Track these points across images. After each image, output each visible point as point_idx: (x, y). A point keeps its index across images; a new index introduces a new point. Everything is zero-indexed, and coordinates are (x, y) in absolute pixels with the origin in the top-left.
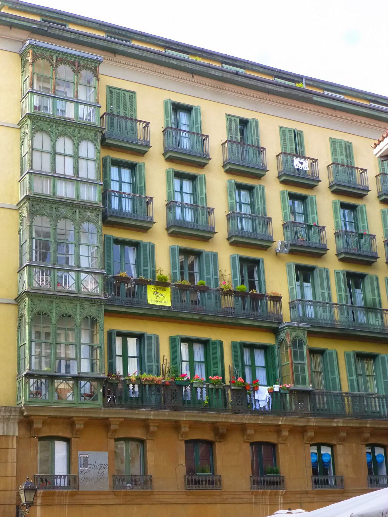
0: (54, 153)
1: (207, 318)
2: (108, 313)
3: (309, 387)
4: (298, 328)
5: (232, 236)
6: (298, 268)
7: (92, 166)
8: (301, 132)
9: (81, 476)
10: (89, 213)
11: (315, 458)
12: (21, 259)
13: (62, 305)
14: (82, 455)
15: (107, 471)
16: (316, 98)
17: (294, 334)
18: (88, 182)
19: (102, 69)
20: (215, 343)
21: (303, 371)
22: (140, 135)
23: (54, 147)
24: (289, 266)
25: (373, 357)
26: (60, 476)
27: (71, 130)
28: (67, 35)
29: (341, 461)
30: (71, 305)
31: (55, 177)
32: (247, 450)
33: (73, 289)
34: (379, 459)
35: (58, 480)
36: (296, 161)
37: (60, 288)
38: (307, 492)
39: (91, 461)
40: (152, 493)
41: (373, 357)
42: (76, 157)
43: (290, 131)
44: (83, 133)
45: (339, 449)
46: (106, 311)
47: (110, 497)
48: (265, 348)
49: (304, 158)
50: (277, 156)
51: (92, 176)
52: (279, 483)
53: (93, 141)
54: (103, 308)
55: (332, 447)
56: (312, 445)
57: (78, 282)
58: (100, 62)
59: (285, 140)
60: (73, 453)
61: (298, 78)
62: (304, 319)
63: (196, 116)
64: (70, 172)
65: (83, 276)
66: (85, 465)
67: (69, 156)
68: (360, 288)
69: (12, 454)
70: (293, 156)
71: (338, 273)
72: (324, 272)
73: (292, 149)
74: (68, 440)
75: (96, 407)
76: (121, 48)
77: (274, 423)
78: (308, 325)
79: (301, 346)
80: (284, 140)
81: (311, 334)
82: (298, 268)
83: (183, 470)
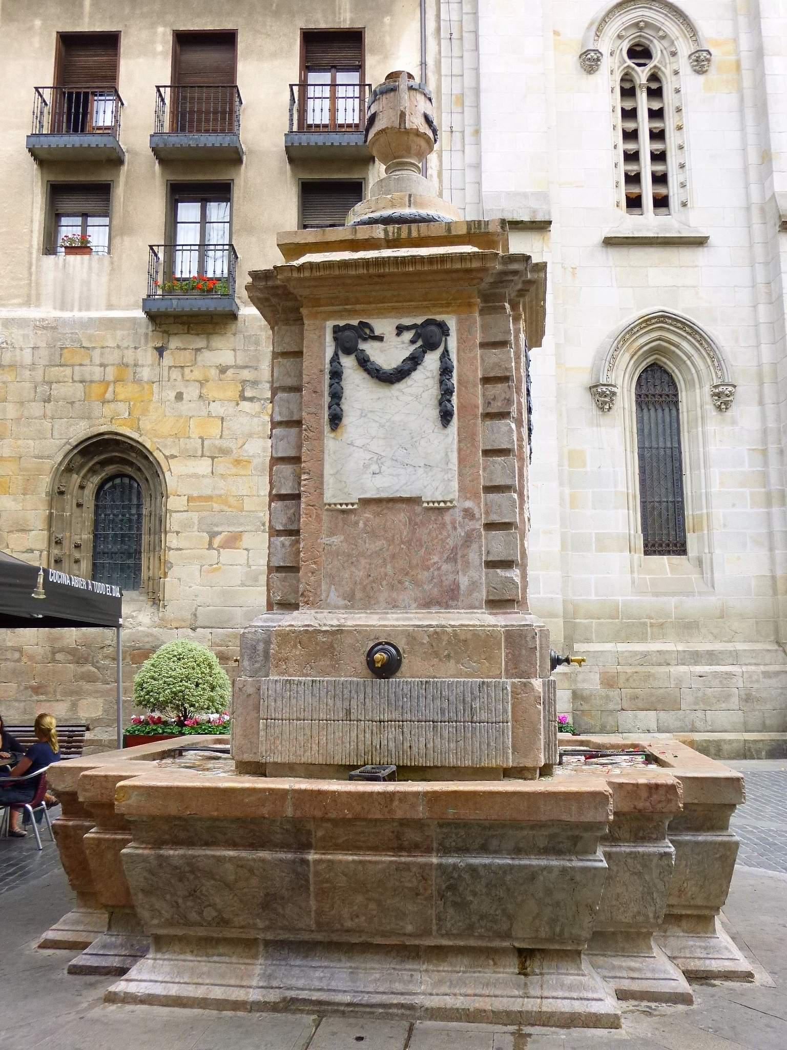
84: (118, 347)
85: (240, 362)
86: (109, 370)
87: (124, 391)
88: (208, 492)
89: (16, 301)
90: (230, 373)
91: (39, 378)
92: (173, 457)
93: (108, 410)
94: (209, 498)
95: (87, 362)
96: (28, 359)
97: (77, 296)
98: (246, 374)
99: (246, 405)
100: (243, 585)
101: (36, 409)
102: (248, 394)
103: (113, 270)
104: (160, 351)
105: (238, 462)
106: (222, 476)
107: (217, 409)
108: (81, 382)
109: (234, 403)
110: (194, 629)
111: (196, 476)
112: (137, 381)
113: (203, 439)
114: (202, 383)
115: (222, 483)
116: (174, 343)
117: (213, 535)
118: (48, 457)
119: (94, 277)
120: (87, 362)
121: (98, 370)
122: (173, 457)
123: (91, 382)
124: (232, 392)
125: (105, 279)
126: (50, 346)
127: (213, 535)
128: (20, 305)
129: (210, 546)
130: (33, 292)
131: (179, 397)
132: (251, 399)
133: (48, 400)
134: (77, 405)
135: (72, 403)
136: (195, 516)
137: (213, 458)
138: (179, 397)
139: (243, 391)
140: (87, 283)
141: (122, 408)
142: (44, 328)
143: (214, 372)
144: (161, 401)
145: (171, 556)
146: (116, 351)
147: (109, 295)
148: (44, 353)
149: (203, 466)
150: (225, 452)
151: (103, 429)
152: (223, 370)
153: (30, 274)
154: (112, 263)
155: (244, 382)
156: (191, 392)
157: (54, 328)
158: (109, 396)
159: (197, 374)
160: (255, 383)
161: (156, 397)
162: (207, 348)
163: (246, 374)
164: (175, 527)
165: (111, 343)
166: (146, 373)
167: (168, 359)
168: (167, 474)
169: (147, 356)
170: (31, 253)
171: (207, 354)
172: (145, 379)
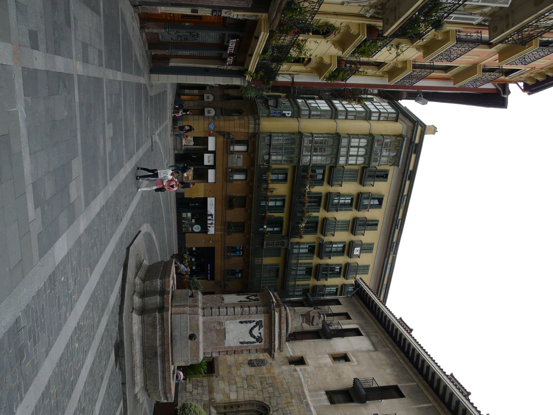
0: (358, 147)
1: (293, 207)
2: (294, 167)
3: (265, 247)
4: (288, 244)
5: (326, 220)
6: (314, 247)
7: (354, 162)
8: (372, 253)
9: (234, 156)
10: (334, 160)
11: (238, 248)
12: (316, 134)
13: (298, 149)
14: (241, 156)
15: (235, 165)
16: (386, 259)
17: (286, 242)
18: (347, 160)
19: (396, 167)
20: (283, 210)
21: (271, 245)
22: (368, 183)
23: (362, 147)
24: (314, 243)
25: (277, 276)
26: (234, 148)
27: (368, 154)
28: (410, 153)
29: (237, 258)
30: (297, 153)
31: (349, 147)
32: (242, 221)
33: (304, 153)
34: (237, 275)
35: (232, 147)
36: (358, 249)
37: (304, 148)
38: (225, 244)
39: (239, 159)
40: (227, 182)
41: (277, 276)
42: (357, 156)
43: (372, 247)
44: (367, 159)
45: (241, 258)
46: (296, 166)
47: (226, 166)
48: (281, 231)
49: (360, 253)
50: (361, 241)
51: (350, 162)
52: (229, 233)
53: (364, 163)
54: (297, 165)
55: (242, 256)
56: (243, 247)
57: (307, 156)
58: (398, 166)
59: (368, 245)
60: (242, 153)
61: (395, 253)
62: (293, 248)
63: (379, 207)
64: (351, 153)
65: (309, 157)
66: (238, 157)
67: (358, 153)
68: (306, 273)
69: (242, 130)
70: (361, 248)
71: (311, 263)
72: (312, 258)
73: (364, 248)
74: (247, 151)
75: (259, 162)
76: (405, 176)
77: (251, 232)
78: (289, 248)
79: (281, 245)
80: (368, 244)
81: (286, 249)
82: (314, 247)
83: (234, 195)
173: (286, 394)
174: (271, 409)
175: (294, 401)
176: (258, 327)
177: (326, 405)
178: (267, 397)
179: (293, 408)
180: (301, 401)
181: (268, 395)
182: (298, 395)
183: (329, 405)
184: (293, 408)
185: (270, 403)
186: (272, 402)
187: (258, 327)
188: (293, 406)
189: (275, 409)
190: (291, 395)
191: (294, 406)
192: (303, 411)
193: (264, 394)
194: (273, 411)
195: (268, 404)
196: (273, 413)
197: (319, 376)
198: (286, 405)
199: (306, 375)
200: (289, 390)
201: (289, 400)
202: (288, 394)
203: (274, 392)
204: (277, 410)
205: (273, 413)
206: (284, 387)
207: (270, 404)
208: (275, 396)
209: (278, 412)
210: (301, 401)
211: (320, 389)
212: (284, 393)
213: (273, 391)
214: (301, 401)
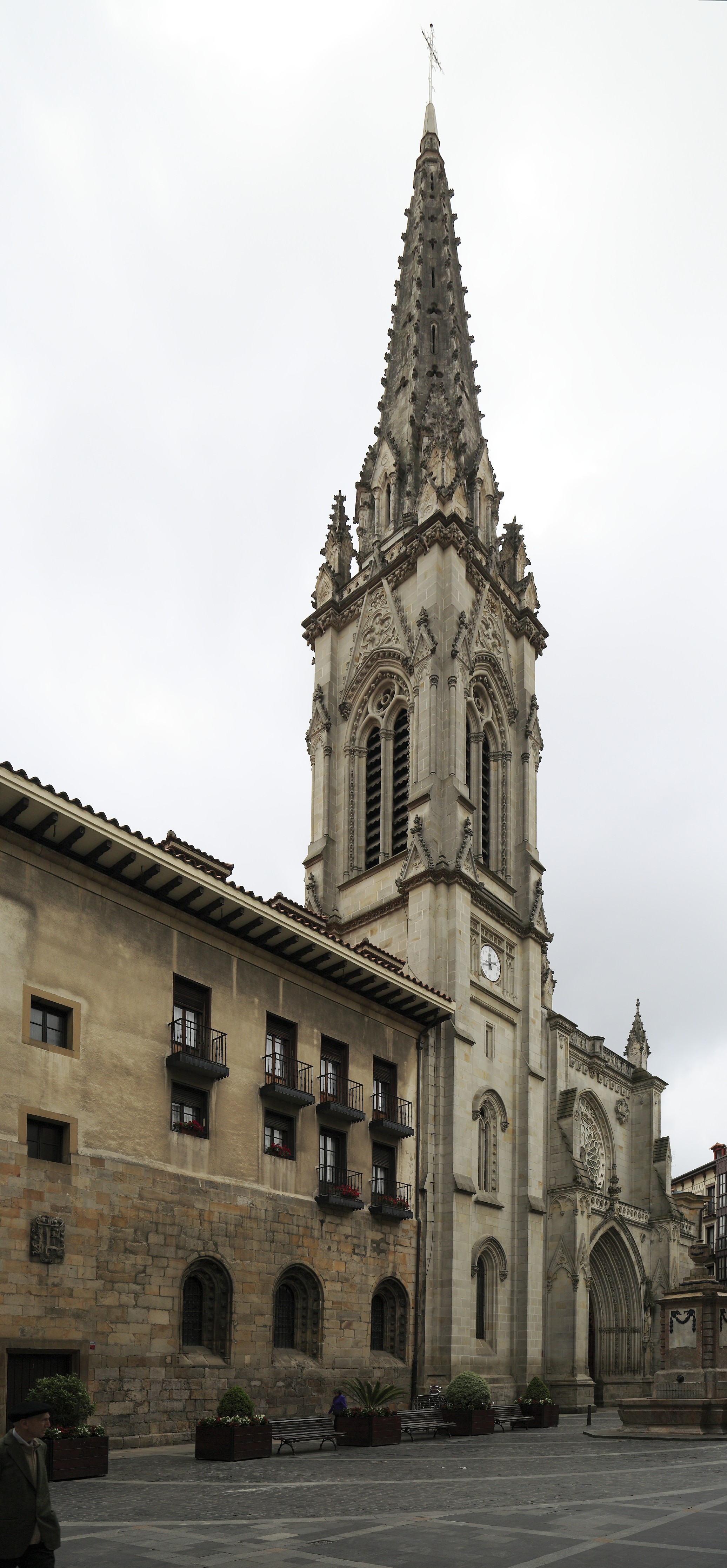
84: (304, 1217)
85: (353, 1234)
86: (301, 1229)
87: (307, 1242)
88: (340, 1300)
89: (252, 1178)
90: (349, 1239)
91: (268, 1229)
92: (327, 1280)
93: (300, 1251)
94: (340, 1303)
95: (290, 1223)
96: (263, 1217)
97: (281, 1182)
98: (355, 1241)
99: (355, 1257)
100: (352, 1347)
101: (267, 1245)
102: (356, 1251)
103: (297, 1170)
104: (322, 1222)
105: (351, 1286)
106: (346, 1293)
107: (345, 1257)
108: (288, 1233)
109: (350, 1255)
110: (333, 1369)
111: (335, 1291)
112: (312, 1237)
113: (338, 1272)
114: (339, 1242)
115: (345, 1296)
116: (328, 1219)
117: (342, 1322)
118: (273, 1274)
119: (289, 1173)
120: (290, 1223)
121: (295, 1228)
122: (327, 1280)
123: (292, 1234)
124: (349, 1250)
125: (294, 1175)
126: (274, 1211)
127: (342, 1322)
128: (254, 1182)
129: (341, 1328)
130: (260, 1175)
131: (329, 1248)
132: (357, 1254)
133: (272, 1241)
134: (286, 1246)
135: (284, 1245)
136: (335, 1312)
137: (342, 1282)
138: (329, 1248)
139: (354, 1250)
140: (285, 1175)
141: (306, 1250)
142: (271, 1199)
143: (343, 1238)
144: (322, 1250)
145: (326, 1332)
146: (304, 1219)
147: (296, 1185)
148: (271, 1214)
149: (338, 1286)
150: (347, 1280)
151: (298, 1261)
152: (347, 1237)
153: (258, 1164)
154: (297, 1166)
155: (354, 1245)
156: (334, 1248)
157: (275, 1200)
158: (300, 1243)
159: (336, 1238)
160: (359, 1246)
161: (319, 1247)
162: (341, 1224)
163: (355, 1241)
164: (327, 1317)
165: (301, 1214)
166: (316, 1233)
167: (325, 1228)
168: (324, 1289)
169: (316, 1224)
170: (258, 1151)
171: (341, 1228)
172: (316, 1236)
173: (176, 1213)
174: (211, 1254)
175: (199, 1205)
176: (678, 1316)
177: (210, 1150)
178: (176, 1252)
179: (216, 1214)
180: (199, 1192)
181: (173, 1249)
182: (183, 1189)
183: (211, 1144)
184: (216, 1214)
185: (193, 1251)
186: (192, 1248)
187: (678, 1316)
188: (211, 1212)
189: (211, 1245)
190: (180, 1203)
191: (212, 1209)
192: (225, 1199)
193: (167, 1255)
194: (217, 1251)
195: (195, 1256)
196: (219, 1253)
197: (119, 1116)
198: (206, 1225)
199: (113, 1143)
200: (166, 1202)
201: (195, 1213)
202: (177, 1210)
203: (164, 1234)
204: (216, 1244)
205: (219, 1253)
206: (154, 1208)
207: (198, 1252)
208: (179, 1236)
209: (219, 1244)
210: (199, 1192)
211: (166, 1136)
212: (173, 1216)
213: (162, 1237)
214: (199, 1192)
